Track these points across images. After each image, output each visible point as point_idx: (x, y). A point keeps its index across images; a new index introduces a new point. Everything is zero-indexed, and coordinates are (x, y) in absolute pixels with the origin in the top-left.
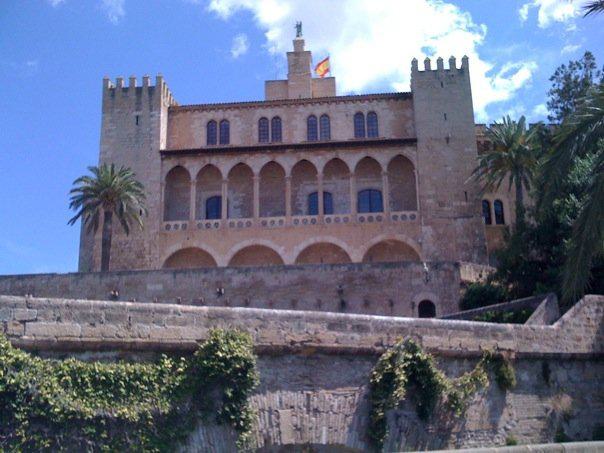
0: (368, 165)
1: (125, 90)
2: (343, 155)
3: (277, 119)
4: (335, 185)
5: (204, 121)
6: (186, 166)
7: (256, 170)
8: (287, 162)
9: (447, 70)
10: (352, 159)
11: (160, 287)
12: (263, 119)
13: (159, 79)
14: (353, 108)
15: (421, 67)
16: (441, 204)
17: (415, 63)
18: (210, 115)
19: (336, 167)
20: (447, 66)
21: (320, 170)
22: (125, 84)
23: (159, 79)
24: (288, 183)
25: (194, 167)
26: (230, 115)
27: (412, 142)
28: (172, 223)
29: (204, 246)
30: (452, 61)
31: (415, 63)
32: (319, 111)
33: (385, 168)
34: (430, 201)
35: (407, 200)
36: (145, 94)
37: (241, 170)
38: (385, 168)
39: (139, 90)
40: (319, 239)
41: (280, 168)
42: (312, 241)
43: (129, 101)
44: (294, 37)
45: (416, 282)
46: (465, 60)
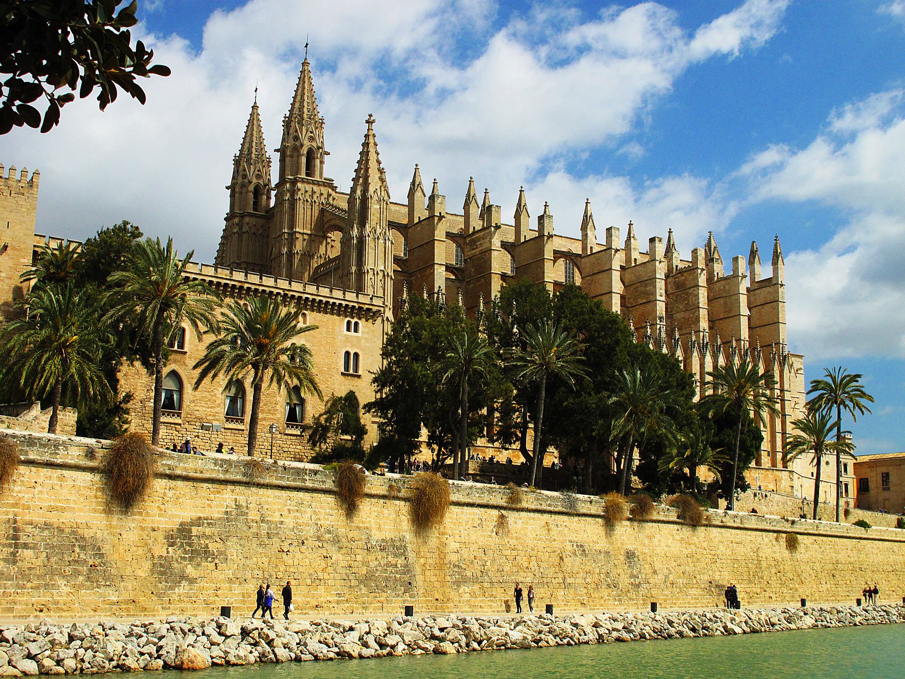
9: (20, 181)
46: (37, 173)
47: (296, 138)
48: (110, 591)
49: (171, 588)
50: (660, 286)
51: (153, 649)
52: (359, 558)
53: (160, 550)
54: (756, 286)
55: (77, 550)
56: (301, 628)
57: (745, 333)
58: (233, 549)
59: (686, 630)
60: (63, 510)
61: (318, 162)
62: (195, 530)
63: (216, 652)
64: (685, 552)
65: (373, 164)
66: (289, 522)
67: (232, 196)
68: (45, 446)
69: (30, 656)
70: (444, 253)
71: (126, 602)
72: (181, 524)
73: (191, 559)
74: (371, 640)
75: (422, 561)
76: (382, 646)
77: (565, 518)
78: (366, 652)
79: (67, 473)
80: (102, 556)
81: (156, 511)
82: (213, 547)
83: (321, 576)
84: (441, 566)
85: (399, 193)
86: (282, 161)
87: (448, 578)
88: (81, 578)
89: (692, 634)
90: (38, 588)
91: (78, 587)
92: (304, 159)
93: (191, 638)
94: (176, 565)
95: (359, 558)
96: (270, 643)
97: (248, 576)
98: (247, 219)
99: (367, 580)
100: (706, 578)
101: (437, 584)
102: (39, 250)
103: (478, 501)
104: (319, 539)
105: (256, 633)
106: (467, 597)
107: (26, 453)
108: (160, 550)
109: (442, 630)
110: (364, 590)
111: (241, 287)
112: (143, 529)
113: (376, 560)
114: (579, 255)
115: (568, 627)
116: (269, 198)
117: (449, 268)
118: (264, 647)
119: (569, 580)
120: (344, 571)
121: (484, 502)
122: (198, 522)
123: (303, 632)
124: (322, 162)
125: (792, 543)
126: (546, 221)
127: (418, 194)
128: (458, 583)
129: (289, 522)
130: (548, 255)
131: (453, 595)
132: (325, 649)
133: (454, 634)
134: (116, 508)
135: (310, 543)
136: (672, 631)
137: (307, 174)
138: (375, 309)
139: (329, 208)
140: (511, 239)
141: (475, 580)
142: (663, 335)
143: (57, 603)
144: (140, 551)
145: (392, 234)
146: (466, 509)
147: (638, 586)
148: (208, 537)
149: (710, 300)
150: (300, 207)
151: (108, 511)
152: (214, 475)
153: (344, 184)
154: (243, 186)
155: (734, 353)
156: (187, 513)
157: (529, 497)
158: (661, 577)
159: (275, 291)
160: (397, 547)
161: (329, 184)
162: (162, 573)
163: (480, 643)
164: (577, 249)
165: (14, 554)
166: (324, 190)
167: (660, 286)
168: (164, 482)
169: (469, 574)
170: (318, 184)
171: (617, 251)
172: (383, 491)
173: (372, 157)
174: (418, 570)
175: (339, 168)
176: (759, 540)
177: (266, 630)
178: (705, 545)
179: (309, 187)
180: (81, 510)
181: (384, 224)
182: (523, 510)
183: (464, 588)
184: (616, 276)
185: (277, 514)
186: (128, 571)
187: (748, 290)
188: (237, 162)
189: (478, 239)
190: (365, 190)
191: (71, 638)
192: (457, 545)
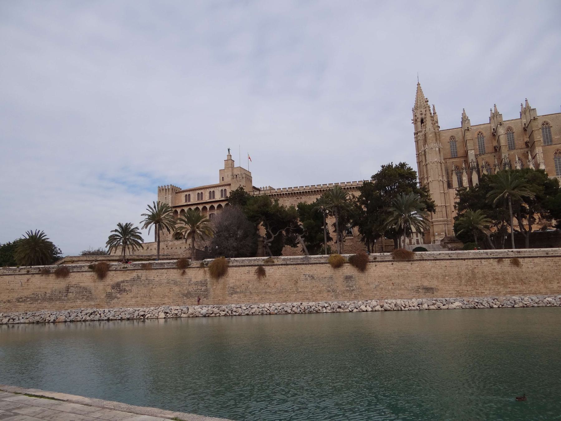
2: (213, 204)
3: (202, 193)
5: (184, 195)
14: (220, 188)
26: (190, 193)
44: (228, 154)
62: (122, 284)
66: (157, 279)
75: (214, 287)
77: (303, 266)
79: (84, 273)
82: (127, 288)
83: (167, 294)
84: (224, 288)
95: (185, 288)
97: (139, 296)
99: (188, 295)
100: (414, 285)
104: (168, 283)
108: (109, 290)
110: (185, 298)
111: (321, 191)
119: (300, 290)
121: (252, 264)
122: (123, 282)
128: (232, 294)
141: (241, 292)
146: (241, 268)
147: (353, 290)
151: (95, 282)
156: (120, 279)
168: (114, 272)
169: (238, 290)
178: (418, 269)
182: (274, 265)
192: (234, 281)
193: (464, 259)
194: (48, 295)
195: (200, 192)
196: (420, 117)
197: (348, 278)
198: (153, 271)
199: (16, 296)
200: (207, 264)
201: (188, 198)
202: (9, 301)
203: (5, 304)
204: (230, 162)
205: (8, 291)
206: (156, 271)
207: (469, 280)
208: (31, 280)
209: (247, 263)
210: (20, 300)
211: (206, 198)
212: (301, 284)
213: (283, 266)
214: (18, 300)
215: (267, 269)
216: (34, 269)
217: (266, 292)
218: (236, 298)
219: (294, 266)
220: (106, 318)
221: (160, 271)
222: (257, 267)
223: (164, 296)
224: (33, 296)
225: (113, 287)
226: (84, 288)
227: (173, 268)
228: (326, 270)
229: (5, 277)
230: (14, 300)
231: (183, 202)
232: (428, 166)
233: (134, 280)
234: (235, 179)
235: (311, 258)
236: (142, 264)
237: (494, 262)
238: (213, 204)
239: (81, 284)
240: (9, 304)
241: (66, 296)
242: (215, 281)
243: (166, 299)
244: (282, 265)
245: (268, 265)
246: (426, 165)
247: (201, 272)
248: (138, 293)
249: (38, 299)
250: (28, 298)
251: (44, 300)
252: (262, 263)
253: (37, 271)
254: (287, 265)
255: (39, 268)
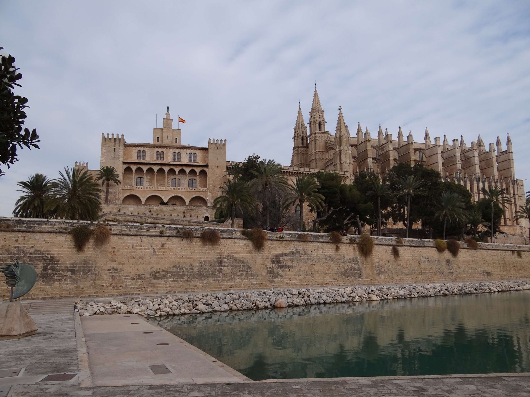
0: (193, 172)
1: (110, 139)
2: (184, 168)
3: (162, 152)
4: (182, 177)
5: (137, 151)
6: (131, 167)
7: (156, 171)
8: (166, 169)
10: (188, 170)
11: (132, 209)
12: (158, 152)
13: (123, 135)
14: (189, 151)
15: (212, 142)
16: (214, 187)
17: (210, 140)
18: (139, 149)
19: (182, 172)
20: (219, 143)
21: (177, 173)
22: (110, 137)
23: (123, 135)
24: (166, 176)
25: (134, 168)
26: (146, 149)
27: (207, 166)
28: (126, 186)
29: (137, 195)
30: (221, 140)
31: (210, 140)
32: (177, 151)
33: (198, 174)
34: (211, 185)
35: (205, 184)
36: (117, 141)
37: (150, 171)
38: (198, 174)
39: (115, 139)
40: (176, 195)
41: (164, 171)
42: (173, 195)
43: (111, 142)
44: (166, 112)
45: (204, 211)
46: (225, 141)
47: (314, 118)
48: (253, 280)
49: (275, 278)
50: (458, 158)
51: (267, 300)
52: (341, 266)
53: (269, 265)
54: (500, 154)
55: (242, 267)
56: (320, 291)
57: (496, 173)
58: (295, 263)
59: (472, 290)
60: (236, 253)
61: (323, 126)
62: (281, 258)
63: (289, 300)
64: (472, 259)
65: (342, 124)
67: (294, 141)
68: (228, 232)
69: (226, 303)
70: (371, 154)
71: (259, 284)
72: (276, 256)
73: (281, 268)
74: (345, 295)
76: (349, 297)
77: (420, 248)
78: (344, 300)
79: (236, 241)
80: (250, 268)
81: (267, 252)
82: (288, 264)
84: (372, 267)
85: (353, 134)
86: (310, 127)
87: (375, 272)
88: (243, 276)
89: (475, 292)
90: (229, 280)
91: (243, 280)
92: (318, 125)
93: (280, 296)
94: (275, 270)
95: (341, 266)
96: (308, 297)
97: (301, 273)
98: (300, 149)
99: (345, 274)
100: (482, 269)
101: (371, 274)
102: (229, 166)
103: (386, 243)
104: (326, 259)
105: (303, 293)
106: (383, 279)
107: (223, 235)
108: (269, 265)
109: (372, 291)
110: (344, 277)
112: (263, 258)
113: (347, 266)
114: (423, 149)
115: (422, 289)
116: (307, 140)
117: (373, 159)
118: (306, 298)
119: (423, 272)
120: (336, 270)
121: (387, 243)
122: (282, 255)
123: (321, 293)
124: (324, 126)
125: (519, 254)
126: (410, 138)
127: (360, 133)
128: (379, 274)
129: (315, 254)
130: (412, 151)
131: (377, 278)
132: (328, 298)
133: (378, 292)
134: (254, 252)
135: (323, 261)
136: (467, 290)
137: (320, 130)
138: (346, 176)
139: (328, 142)
140: (397, 146)
141: (386, 272)
142: (461, 176)
143: (236, 285)
144: (263, 266)
145: (351, 149)
146: (380, 247)
147: (453, 273)
148: (286, 260)
149: (480, 161)
150: (317, 142)
151: (251, 253)
152: (287, 239)
153: (333, 132)
154: (298, 137)
155: (492, 182)
157: (406, 240)
158: (462, 269)
159: (309, 173)
160: (355, 261)
161: (328, 133)
162: (271, 273)
163: (387, 295)
164: (423, 147)
165: (221, 269)
166: (326, 135)
167: (458, 158)
169: (383, 270)
170: (323, 133)
171: (439, 146)
172: (348, 241)
173: (342, 121)
174: (363, 269)
175: (331, 127)
176: (504, 254)
177: (307, 293)
179: (320, 135)
180: (242, 253)
181: (348, 145)
182: (403, 246)
183: (381, 275)
184: (440, 155)
185: (310, 251)
186: (259, 273)
187: (497, 156)
188: (295, 129)
189: (384, 147)
190: (340, 134)
191: (240, 297)
192: (378, 260)
193: (499, 250)
194: (196, 269)
195: (160, 150)
196: (319, 120)
197: (448, 261)
198: (310, 244)
199: (149, 269)
200: (355, 240)
201: (141, 154)
202: (139, 277)
203: (133, 282)
204: (167, 120)
205: (134, 261)
206: (312, 244)
207: (504, 267)
208: (167, 246)
209: (384, 242)
210: (157, 275)
211: (169, 158)
212: (423, 265)
213: (408, 248)
214: (154, 275)
215: (399, 248)
216: (170, 229)
217: (402, 273)
218: (383, 279)
219: (415, 248)
220: (322, 301)
221: (315, 244)
222: (391, 247)
223: (326, 275)
224: (174, 269)
225: (273, 262)
226: (240, 261)
227: (326, 242)
228: (433, 253)
229: (125, 238)
230: (148, 276)
231: (135, 159)
232: (343, 165)
233: (292, 253)
234: (213, 145)
235: (424, 241)
236: (298, 234)
237: (510, 253)
238: (184, 168)
239: (236, 256)
240: (140, 282)
241: (221, 271)
242: (364, 259)
243: (328, 277)
244: (407, 246)
245: (399, 246)
246: (341, 164)
247: (351, 248)
248: (300, 270)
249: (183, 276)
250: (168, 272)
251: (192, 275)
252: (394, 243)
253: (174, 233)
254: (411, 246)
255: (177, 228)
